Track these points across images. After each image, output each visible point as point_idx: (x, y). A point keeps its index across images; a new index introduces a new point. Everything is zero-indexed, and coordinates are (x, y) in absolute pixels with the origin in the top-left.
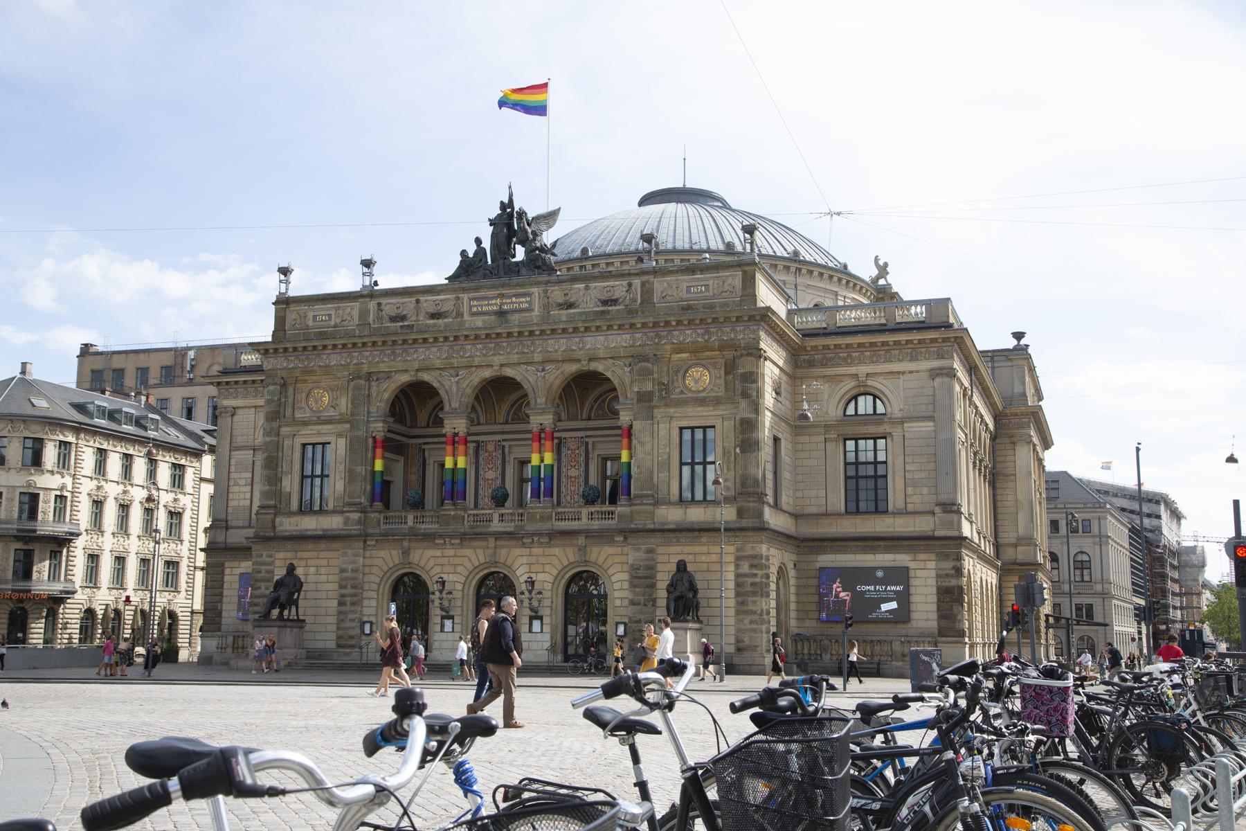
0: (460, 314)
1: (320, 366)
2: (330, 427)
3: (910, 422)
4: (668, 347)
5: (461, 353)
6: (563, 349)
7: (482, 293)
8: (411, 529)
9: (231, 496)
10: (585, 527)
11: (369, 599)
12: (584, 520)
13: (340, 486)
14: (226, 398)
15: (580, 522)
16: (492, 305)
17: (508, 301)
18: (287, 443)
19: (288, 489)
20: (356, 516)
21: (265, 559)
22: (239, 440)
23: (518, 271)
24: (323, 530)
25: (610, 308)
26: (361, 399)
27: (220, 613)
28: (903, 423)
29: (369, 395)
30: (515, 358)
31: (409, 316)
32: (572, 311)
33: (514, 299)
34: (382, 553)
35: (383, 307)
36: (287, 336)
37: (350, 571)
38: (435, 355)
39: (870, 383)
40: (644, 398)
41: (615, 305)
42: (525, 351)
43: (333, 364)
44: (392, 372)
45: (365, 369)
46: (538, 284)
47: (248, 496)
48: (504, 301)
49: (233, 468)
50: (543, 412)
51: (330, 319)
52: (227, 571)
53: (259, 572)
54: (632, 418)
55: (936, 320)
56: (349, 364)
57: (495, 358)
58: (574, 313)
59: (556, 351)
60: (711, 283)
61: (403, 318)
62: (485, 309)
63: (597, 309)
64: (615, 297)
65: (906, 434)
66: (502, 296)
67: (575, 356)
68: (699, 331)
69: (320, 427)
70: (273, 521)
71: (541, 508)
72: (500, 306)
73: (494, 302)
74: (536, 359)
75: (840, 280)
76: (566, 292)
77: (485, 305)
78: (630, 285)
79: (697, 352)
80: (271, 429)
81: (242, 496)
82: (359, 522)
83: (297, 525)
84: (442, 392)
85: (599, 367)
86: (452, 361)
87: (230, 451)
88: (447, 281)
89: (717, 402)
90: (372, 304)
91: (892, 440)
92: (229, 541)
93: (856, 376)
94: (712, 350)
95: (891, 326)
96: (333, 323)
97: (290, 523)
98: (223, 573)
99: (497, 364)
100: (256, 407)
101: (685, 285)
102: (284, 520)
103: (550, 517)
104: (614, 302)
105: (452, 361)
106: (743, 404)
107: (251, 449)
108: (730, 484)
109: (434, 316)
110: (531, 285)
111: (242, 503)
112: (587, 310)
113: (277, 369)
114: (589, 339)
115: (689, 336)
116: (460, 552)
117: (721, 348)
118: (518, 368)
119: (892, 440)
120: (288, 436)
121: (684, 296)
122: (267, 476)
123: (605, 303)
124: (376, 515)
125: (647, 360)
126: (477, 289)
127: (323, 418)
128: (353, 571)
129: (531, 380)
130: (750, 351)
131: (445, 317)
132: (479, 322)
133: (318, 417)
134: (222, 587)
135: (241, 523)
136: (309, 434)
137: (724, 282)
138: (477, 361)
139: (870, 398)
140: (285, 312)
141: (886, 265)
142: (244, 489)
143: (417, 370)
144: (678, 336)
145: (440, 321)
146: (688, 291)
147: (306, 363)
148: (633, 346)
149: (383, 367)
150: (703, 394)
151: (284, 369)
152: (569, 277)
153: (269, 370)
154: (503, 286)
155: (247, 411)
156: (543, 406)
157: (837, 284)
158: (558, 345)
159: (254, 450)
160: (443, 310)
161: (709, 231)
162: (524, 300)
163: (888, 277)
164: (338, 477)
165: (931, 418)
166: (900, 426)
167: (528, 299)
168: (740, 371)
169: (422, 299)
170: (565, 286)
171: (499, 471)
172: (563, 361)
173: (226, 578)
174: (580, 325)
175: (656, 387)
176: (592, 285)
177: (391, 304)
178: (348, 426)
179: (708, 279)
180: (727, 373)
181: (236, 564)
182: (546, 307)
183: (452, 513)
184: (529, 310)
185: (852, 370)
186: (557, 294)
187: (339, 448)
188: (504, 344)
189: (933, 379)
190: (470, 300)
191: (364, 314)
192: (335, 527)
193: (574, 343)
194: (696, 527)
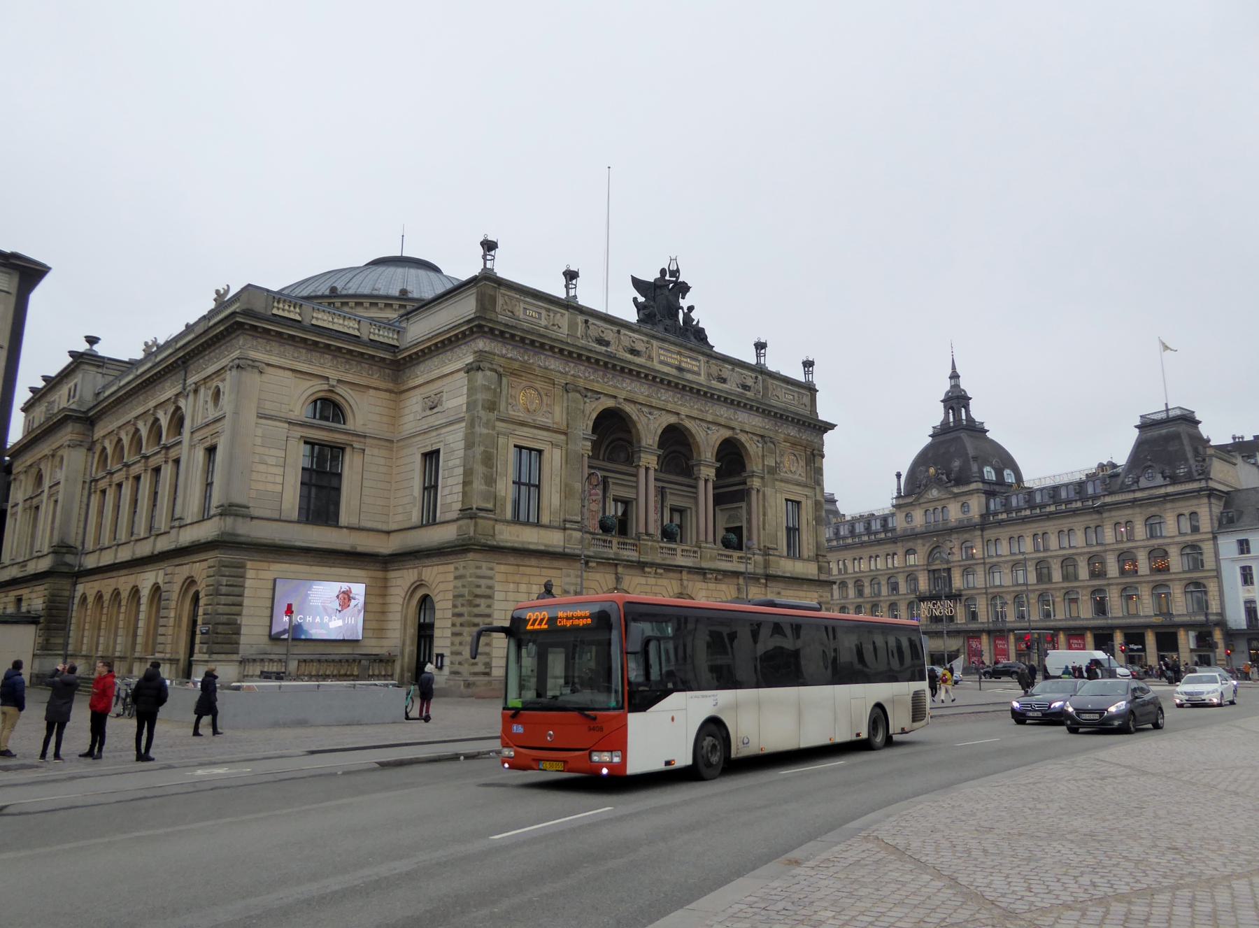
0: (650, 358)
1: (540, 366)
2: (545, 433)
7: (666, 345)
8: (616, 554)
13: (556, 500)
14: (256, 349)
16: (674, 358)
17: (685, 360)
18: (501, 440)
19: (503, 494)
21: (484, 572)
22: (269, 408)
24: (545, 546)
27: (240, 625)
30: (695, 413)
34: (598, 576)
37: (572, 592)
38: (641, 391)
44: (602, 393)
46: (704, 354)
47: (279, 479)
52: (250, 574)
53: (479, 586)
56: (566, 373)
61: (607, 344)
62: (669, 360)
66: (679, 353)
67: (733, 424)
69: (536, 431)
70: (494, 528)
78: (756, 378)
80: (488, 421)
81: (270, 478)
83: (518, 536)
90: (580, 319)
96: (543, 322)
97: (510, 533)
98: (243, 577)
100: (293, 371)
102: (504, 527)
107: (286, 422)
108: (811, 547)
109: (633, 352)
111: (270, 487)
113: (495, 354)
115: (793, 431)
116: (660, 581)
118: (693, 422)
120: (505, 435)
122: (484, 474)
126: (663, 340)
127: (538, 422)
132: (666, 369)
133: (534, 420)
134: (241, 595)
135: (268, 514)
136: (527, 437)
138: (670, 407)
140: (495, 292)
143: (624, 399)
150: (796, 477)
151: (503, 356)
155: (281, 372)
164: (553, 490)
169: (623, 331)
171: (601, 505)
173: (248, 583)
176: (737, 369)
178: (563, 437)
181: (265, 565)
183: (650, 543)
191: (572, 325)
192: (555, 543)
194: (800, 576)
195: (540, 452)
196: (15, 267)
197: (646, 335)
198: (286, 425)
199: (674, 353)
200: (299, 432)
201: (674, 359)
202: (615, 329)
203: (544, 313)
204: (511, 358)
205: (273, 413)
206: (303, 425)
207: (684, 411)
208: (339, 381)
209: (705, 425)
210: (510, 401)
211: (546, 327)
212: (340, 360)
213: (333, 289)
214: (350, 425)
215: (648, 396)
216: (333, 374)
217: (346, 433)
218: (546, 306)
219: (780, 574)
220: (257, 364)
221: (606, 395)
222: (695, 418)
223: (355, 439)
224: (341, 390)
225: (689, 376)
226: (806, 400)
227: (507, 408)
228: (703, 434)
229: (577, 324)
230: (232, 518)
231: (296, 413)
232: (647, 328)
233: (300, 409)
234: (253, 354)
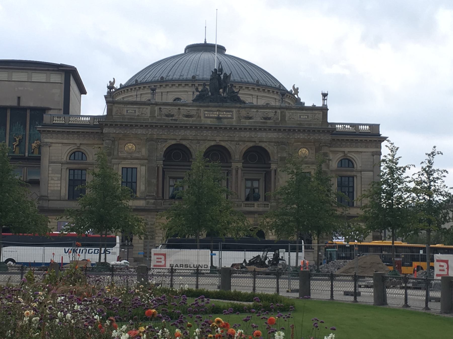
2: (137, 161)
3: (364, 172)
4: (293, 140)
5: (202, 134)
6: (248, 136)
7: (210, 109)
9: (49, 185)
10: (256, 210)
11: (159, 237)
12: (256, 207)
14: (46, 138)
15: (254, 208)
16: (214, 114)
17: (222, 113)
18: (115, 167)
20: (153, 201)
23: (226, 101)
24: (136, 206)
25: (267, 121)
28: (361, 172)
29: (157, 148)
30: (226, 138)
31: (175, 115)
32: (251, 120)
33: (225, 113)
35: (161, 110)
36: (114, 118)
37: (150, 224)
38: (190, 134)
39: (349, 155)
40: (282, 159)
41: (269, 120)
42: (231, 135)
43: (139, 133)
44: (168, 139)
45: (155, 137)
46: (236, 107)
47: (59, 185)
48: (220, 113)
49: (50, 172)
50: (239, 162)
51: (135, 112)
54: (277, 167)
55: (374, 132)
56: (147, 134)
57: (217, 137)
58: (251, 121)
59: (245, 137)
60: (309, 115)
61: (172, 116)
62: (211, 115)
63: (261, 121)
64: (269, 117)
65: (362, 177)
66: (218, 111)
68: (305, 134)
69: (132, 161)
71: (237, 201)
72: (218, 115)
73: (215, 113)
74: (236, 140)
75: (277, 93)
76: (248, 112)
77: (211, 114)
78: (276, 112)
79: (305, 143)
81: (56, 185)
82: (154, 204)
84: (191, 150)
85: (263, 145)
86: (197, 137)
87: (49, 163)
88: (192, 102)
90: (157, 108)
91: (357, 178)
92: (49, 206)
93: (344, 152)
95: (357, 133)
96: (137, 114)
99: (219, 140)
100: (62, 143)
101: (299, 115)
103: (241, 205)
104: (270, 119)
105: (197, 137)
107: (60, 163)
109: (187, 116)
110: (233, 107)
111: (56, 188)
112: (257, 121)
113: (110, 133)
114: (259, 133)
115: (302, 136)
118: (227, 142)
119: (357, 178)
120: (116, 164)
121: (298, 119)
123: (265, 118)
124: (161, 201)
125: (285, 145)
126: (208, 106)
127: (133, 157)
128: (151, 225)
129: (232, 147)
130: (327, 144)
131: (192, 117)
132: (209, 121)
133: (131, 156)
135: (56, 198)
136: (127, 164)
137: (315, 115)
139: (347, 161)
141: (298, 89)
142: (56, 182)
143: (180, 139)
144: (297, 136)
145: (190, 118)
146: (300, 117)
147: (125, 132)
148: (277, 138)
149: (164, 137)
151: (114, 133)
152: (249, 106)
153: (106, 133)
154: (219, 107)
156: (238, 159)
157: (272, 94)
158: (246, 135)
159: (62, 164)
160: (191, 114)
161: (245, 73)
162: (229, 113)
163: (299, 94)
164: (141, 183)
165: (372, 171)
166: (360, 173)
167: (231, 113)
168: (322, 152)
169: (181, 108)
170: (247, 110)
172: (247, 141)
174: (257, 128)
175: (288, 155)
176: (260, 110)
177: (166, 108)
178: (146, 161)
179: (308, 113)
180: (316, 152)
182: (239, 118)
184: (232, 118)
185: (342, 149)
186: (244, 113)
187: (142, 171)
188: (221, 132)
189: (373, 156)
190: (205, 111)
191: (152, 112)
192: (141, 205)
193: (253, 134)
195: (137, 168)
196: (63, 71)
197: (197, 106)
198: (61, 165)
199: (214, 111)
200: (66, 166)
201: (215, 114)
203: (137, 110)
204: (118, 133)
205: (55, 161)
206: (68, 163)
207: (218, 139)
208: (80, 144)
209: (235, 143)
210: (120, 150)
211: (138, 116)
212: (80, 135)
213: (136, 81)
214: (88, 161)
215: (194, 135)
216: (78, 142)
217: (86, 164)
218: (138, 107)
220: (47, 144)
221: (170, 139)
222: (227, 141)
223: (89, 166)
224: (82, 147)
225: (225, 122)
226: (320, 115)
227: (118, 154)
228: (233, 147)
229: (155, 111)
230: (41, 201)
231: (64, 159)
232: (198, 104)
233: (65, 158)
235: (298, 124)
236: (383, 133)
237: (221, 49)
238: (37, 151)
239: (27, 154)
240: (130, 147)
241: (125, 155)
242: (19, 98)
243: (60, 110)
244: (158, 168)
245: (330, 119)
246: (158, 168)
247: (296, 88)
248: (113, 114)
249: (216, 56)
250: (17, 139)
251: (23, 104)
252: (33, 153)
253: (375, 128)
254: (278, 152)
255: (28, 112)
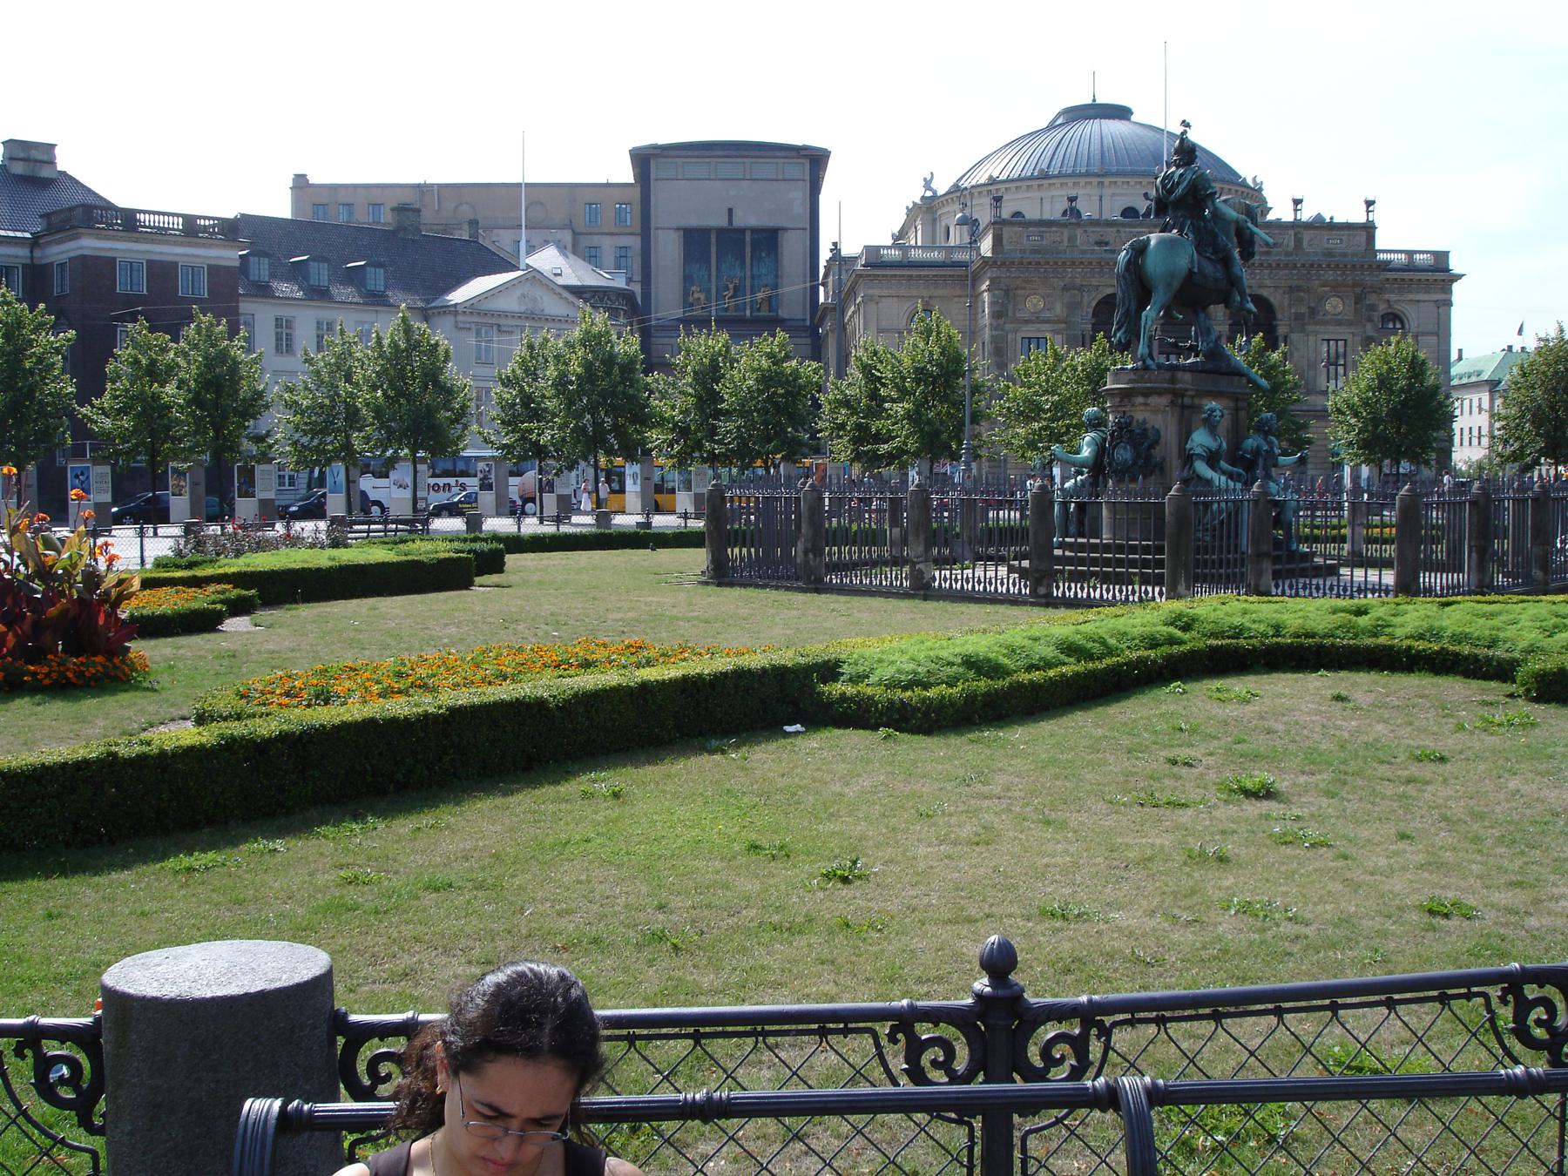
18: (1010, 336)
22: (884, 324)
26: (1073, 306)
40: (1298, 317)
61: (1107, 244)
79: (1336, 289)
89: (1350, 323)
90: (1079, 231)
94: (1347, 286)
106: (1369, 326)
115: (1330, 276)
117: (1354, 286)
155: (890, 300)
169: (1122, 229)
191: (1072, 239)
196: (805, 156)
202: (1115, 229)
216: (926, 293)
219: (1305, 408)
226: (1361, 237)
234: (870, 292)
235: (1324, 255)
236: (1455, 265)
237: (1122, 113)
238: (765, 307)
239: (748, 313)
240: (1035, 301)
241: (1027, 316)
242: (730, 211)
243: (805, 229)
244: (1083, 336)
245: (1381, 242)
246: (1083, 336)
247: (1258, 181)
248: (1005, 242)
249: (1113, 127)
250: (731, 286)
251: (738, 222)
252: (759, 310)
253: (1441, 258)
254: (1290, 305)
255: (748, 234)
